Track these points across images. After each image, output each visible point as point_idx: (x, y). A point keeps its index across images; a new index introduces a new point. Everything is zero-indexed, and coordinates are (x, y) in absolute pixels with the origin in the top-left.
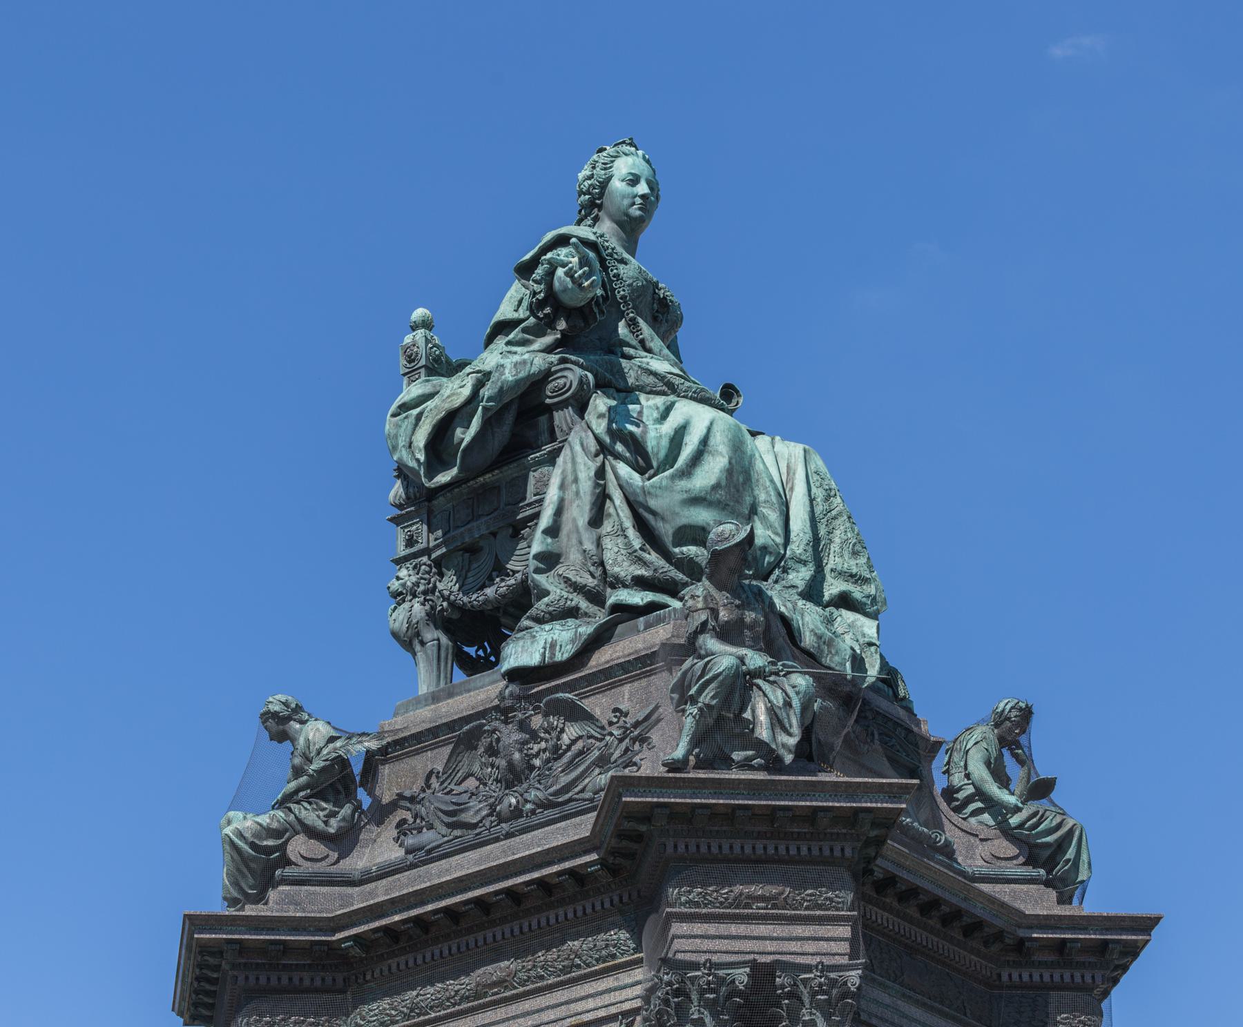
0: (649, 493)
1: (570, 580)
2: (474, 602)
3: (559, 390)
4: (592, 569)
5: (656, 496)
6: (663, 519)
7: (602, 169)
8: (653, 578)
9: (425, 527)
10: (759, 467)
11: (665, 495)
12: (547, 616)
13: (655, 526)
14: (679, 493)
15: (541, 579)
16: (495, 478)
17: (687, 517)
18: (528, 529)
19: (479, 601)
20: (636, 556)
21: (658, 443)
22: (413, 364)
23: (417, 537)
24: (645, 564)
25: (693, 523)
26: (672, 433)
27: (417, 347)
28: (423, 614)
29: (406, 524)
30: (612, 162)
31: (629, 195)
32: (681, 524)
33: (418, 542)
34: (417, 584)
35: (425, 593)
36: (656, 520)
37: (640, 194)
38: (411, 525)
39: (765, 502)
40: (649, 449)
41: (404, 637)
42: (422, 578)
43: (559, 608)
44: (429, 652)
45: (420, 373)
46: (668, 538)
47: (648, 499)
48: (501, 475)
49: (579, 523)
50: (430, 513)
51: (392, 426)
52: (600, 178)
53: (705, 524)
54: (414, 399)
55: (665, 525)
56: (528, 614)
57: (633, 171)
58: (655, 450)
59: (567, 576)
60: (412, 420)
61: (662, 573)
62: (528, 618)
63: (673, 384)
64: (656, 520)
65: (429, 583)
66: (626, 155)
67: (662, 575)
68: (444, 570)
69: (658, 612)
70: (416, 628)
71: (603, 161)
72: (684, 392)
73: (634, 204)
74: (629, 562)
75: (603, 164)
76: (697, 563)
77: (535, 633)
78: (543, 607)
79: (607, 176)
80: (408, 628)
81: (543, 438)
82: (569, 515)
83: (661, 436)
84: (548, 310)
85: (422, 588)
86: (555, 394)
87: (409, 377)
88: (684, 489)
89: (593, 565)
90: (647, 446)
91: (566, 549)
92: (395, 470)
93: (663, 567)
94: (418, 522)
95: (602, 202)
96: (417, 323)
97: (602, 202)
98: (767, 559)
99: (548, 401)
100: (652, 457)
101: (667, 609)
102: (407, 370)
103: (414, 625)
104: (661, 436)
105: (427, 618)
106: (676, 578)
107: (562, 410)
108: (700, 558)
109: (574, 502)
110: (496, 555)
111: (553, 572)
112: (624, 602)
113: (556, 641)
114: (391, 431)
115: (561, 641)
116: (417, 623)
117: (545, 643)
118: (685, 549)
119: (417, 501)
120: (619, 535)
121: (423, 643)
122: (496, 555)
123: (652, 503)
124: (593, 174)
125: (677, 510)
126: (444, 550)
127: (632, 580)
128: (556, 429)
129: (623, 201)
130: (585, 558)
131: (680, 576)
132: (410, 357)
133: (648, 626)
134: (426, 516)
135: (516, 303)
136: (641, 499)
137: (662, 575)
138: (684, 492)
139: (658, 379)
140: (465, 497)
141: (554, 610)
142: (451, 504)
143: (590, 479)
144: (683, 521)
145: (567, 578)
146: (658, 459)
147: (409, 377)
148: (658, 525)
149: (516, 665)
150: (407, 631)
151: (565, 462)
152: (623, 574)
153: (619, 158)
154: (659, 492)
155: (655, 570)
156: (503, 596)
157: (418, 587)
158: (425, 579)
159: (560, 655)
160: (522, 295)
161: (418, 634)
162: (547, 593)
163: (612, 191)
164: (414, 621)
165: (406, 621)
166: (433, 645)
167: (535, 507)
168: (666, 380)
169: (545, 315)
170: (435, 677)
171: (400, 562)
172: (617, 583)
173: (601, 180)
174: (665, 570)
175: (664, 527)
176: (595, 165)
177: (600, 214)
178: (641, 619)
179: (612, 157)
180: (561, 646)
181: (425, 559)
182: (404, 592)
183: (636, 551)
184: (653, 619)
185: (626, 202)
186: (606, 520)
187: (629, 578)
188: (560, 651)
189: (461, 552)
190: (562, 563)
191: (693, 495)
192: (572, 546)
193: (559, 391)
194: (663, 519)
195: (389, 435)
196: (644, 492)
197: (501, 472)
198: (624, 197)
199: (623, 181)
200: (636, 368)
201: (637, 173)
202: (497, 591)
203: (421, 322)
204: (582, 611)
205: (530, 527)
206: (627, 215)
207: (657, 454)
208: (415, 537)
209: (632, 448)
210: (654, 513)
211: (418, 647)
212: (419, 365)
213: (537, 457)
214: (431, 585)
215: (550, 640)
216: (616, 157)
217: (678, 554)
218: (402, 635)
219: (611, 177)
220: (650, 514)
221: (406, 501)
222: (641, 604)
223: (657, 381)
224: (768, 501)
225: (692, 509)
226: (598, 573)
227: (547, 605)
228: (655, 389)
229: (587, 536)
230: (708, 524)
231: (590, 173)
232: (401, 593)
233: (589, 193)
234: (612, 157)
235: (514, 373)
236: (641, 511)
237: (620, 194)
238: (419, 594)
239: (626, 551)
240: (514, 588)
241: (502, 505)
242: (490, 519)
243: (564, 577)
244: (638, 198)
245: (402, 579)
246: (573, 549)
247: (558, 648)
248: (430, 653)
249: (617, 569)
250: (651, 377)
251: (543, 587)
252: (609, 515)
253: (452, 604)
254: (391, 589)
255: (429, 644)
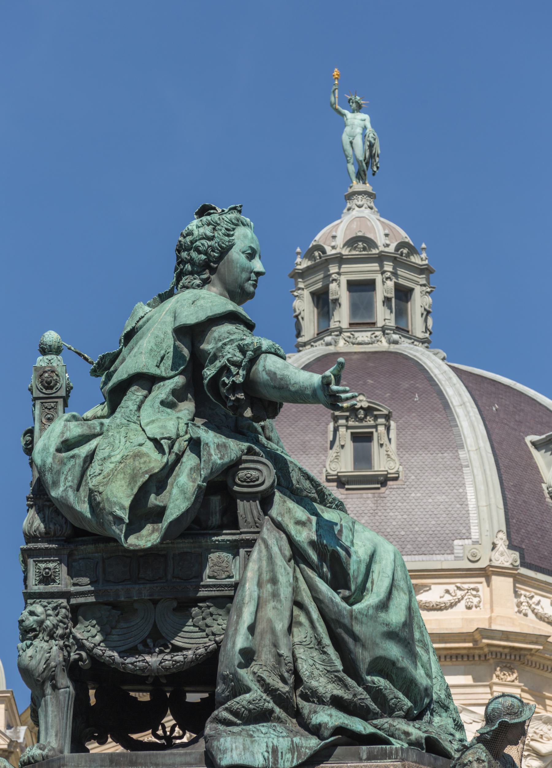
0: (356, 618)
1: (264, 680)
2: (130, 665)
3: (252, 481)
4: (286, 675)
5: (362, 623)
6: (364, 646)
7: (225, 235)
8: (350, 702)
9: (64, 568)
10: (415, 606)
11: (369, 624)
12: (246, 712)
13: (354, 651)
14: (381, 624)
15: (242, 672)
16: (163, 546)
17: (384, 650)
18: (197, 608)
19: (136, 666)
20: (336, 676)
21: (358, 568)
22: (49, 391)
23: (55, 576)
24: (346, 686)
25: (388, 657)
26: (368, 560)
27: (57, 375)
28: (61, 659)
29: (41, 559)
30: (234, 229)
31: (248, 269)
32: (378, 656)
33: (55, 582)
34: (56, 627)
35: (62, 637)
36: (356, 645)
37: (256, 270)
38: (50, 561)
39: (418, 641)
40: (351, 572)
41: (39, 676)
42: (61, 621)
43: (258, 707)
44: (61, 698)
45: (57, 402)
46: (363, 667)
47: (353, 623)
48: (170, 545)
49: (276, 626)
50: (70, 555)
51: (57, 461)
52: (223, 243)
53: (396, 660)
54: (75, 438)
55: (364, 652)
56: (226, 705)
57: (253, 246)
58: (356, 573)
59: (262, 675)
60: (80, 461)
61: (360, 699)
62: (226, 709)
63: (324, 494)
64: (356, 645)
65: (66, 628)
66: (244, 225)
67: (359, 701)
68: (80, 618)
69: (384, 746)
70: (54, 671)
71: (226, 227)
72: (330, 503)
73: (249, 279)
74: (326, 679)
75: (227, 229)
76: (384, 695)
77: (251, 732)
78: (245, 703)
79: (230, 244)
80: (45, 669)
81: (214, 519)
82: (263, 613)
83: (360, 561)
84: (241, 396)
85: (60, 631)
86: (245, 484)
87: (42, 403)
88: (385, 622)
89: (288, 672)
90: (350, 569)
91: (259, 646)
92: (28, 499)
93: (361, 694)
94: (56, 561)
95: (217, 267)
96: (52, 347)
97: (217, 267)
98: (425, 701)
99: (236, 488)
100: (352, 579)
101: (388, 747)
102: (42, 395)
103: (52, 668)
104: (360, 561)
105: (64, 663)
106: (370, 707)
107: (248, 501)
108: (388, 691)
109: (269, 603)
110: (155, 625)
111: (249, 668)
112: (349, 727)
113: (277, 747)
114: (55, 466)
115: (282, 749)
116: (55, 667)
117: (267, 746)
118: (376, 679)
119: (55, 538)
120: (313, 648)
121: (55, 688)
122: (155, 625)
123: (357, 628)
124: (214, 236)
125: (378, 640)
126: (91, 599)
127: (331, 699)
128: (240, 518)
129: (242, 273)
130: (279, 663)
131: (373, 706)
132: (49, 383)
133: (371, 757)
134: (66, 557)
135: (159, 359)
136: (346, 621)
137: (359, 701)
138: (385, 626)
139: (312, 485)
140: (120, 554)
141: (254, 709)
142: (100, 554)
143: (290, 585)
144: (380, 652)
145: (261, 677)
146: (356, 583)
147: (42, 403)
148: (357, 650)
149: (241, 762)
150: (43, 672)
151: (260, 559)
152: (321, 690)
153: (238, 227)
154: (364, 619)
155: (355, 695)
156: (166, 669)
157: (57, 629)
158: (64, 623)
159: (282, 761)
160: (163, 352)
161: (53, 678)
162: (248, 690)
163: (233, 261)
164: (53, 664)
165: (43, 661)
166: (66, 692)
167: (212, 591)
168: (319, 488)
169: (237, 399)
170: (64, 725)
171: (29, 596)
172: (313, 697)
173: (225, 246)
174: (363, 697)
175: (362, 654)
176: (215, 226)
177: (212, 277)
178: (364, 747)
179: (233, 224)
180: (282, 753)
181: (64, 602)
182: (38, 629)
183: (338, 671)
184: (377, 752)
185: (244, 276)
186: (295, 627)
187: (329, 695)
188: (282, 759)
189: (110, 607)
190: (256, 661)
191: (391, 630)
192: (265, 646)
193: (250, 482)
194: (364, 646)
195: (51, 469)
196: (351, 616)
197: (172, 543)
198: (243, 269)
199: (243, 253)
200: (297, 470)
201: (255, 248)
202: (161, 663)
203: (56, 347)
204: (276, 715)
205: (200, 608)
206: (242, 288)
207: (357, 578)
208: (52, 577)
209: (329, 564)
210: (356, 638)
211: (49, 690)
212: (58, 394)
213: (218, 541)
214: (68, 630)
215: (270, 745)
216: (237, 225)
217: (368, 682)
218: (37, 674)
219: (233, 245)
220: (350, 637)
221: (43, 535)
222: (364, 732)
223: (311, 487)
224: (421, 641)
225: (387, 642)
226: (291, 680)
227: (249, 702)
228: (310, 495)
229: (285, 642)
230: (398, 660)
231: (212, 234)
232: (34, 630)
233: (206, 253)
234: (233, 224)
235: (219, 456)
236: (340, 630)
237: (240, 266)
238: (57, 636)
239: (323, 667)
240: (181, 665)
241: (169, 577)
242: (157, 587)
243: (259, 676)
244: (253, 274)
245: (38, 616)
246: (265, 649)
247: (280, 754)
248: (63, 700)
249: (314, 683)
250: (308, 482)
251: (245, 683)
252: (300, 624)
253: (92, 657)
254: (24, 624)
255: (62, 690)
